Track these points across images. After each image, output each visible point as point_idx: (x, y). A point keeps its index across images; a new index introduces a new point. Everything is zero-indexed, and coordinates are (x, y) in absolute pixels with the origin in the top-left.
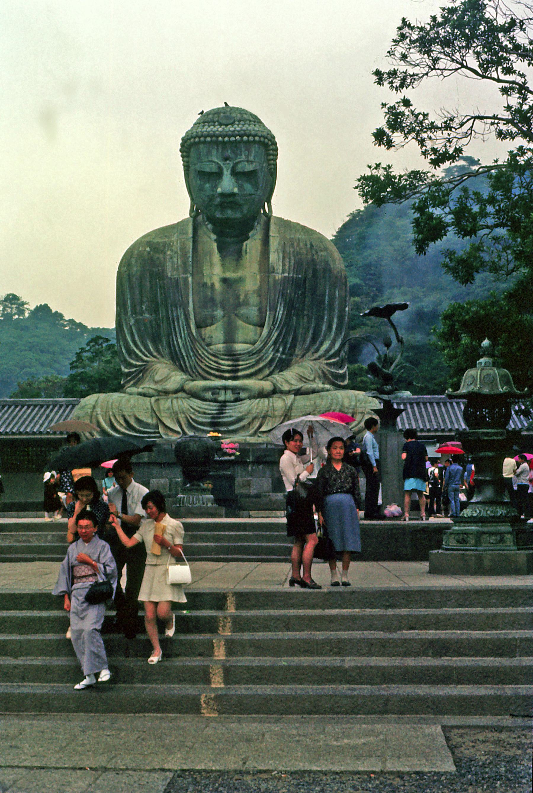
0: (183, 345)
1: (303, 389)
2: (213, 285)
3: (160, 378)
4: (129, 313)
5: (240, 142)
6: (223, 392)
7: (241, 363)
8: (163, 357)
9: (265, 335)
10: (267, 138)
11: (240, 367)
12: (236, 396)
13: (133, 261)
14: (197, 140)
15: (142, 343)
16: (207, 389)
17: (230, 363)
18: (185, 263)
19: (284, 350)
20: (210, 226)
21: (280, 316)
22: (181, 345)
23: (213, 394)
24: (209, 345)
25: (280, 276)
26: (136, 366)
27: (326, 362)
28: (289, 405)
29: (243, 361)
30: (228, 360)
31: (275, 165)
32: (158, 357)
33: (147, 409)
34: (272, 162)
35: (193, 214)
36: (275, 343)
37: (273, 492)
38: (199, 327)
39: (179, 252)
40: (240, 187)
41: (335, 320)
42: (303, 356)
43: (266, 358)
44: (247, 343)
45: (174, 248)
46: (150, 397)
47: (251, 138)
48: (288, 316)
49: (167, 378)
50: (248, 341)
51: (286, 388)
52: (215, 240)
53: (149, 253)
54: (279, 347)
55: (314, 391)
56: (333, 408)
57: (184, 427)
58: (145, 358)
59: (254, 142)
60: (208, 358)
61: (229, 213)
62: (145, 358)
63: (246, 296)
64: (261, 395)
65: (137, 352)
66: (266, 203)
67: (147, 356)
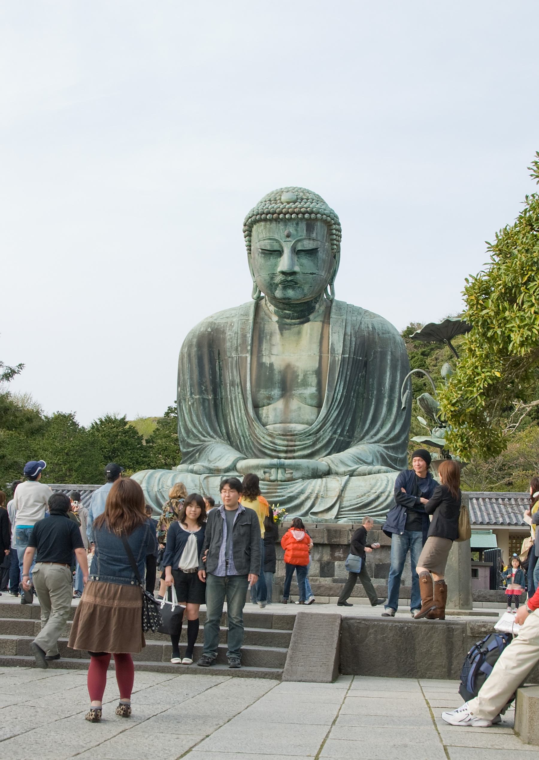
0: (239, 424)
1: (359, 470)
2: (271, 365)
3: (214, 458)
4: (189, 394)
5: (301, 219)
6: (273, 471)
8: (220, 437)
9: (323, 416)
10: (329, 216)
11: (296, 448)
13: (195, 340)
14: (258, 217)
17: (285, 443)
19: (342, 431)
20: (272, 308)
21: (339, 397)
23: (265, 473)
24: (264, 425)
25: (340, 357)
26: (194, 446)
27: (385, 445)
28: (342, 485)
29: (300, 441)
30: (284, 440)
31: (339, 246)
33: (196, 486)
34: (335, 242)
35: (255, 296)
36: (333, 424)
37: (321, 577)
39: (239, 332)
40: (301, 265)
41: (396, 404)
43: (323, 439)
44: (303, 423)
46: (201, 474)
47: (313, 216)
48: (347, 398)
49: (220, 458)
50: (305, 421)
51: (342, 469)
52: (277, 322)
53: (210, 333)
54: (336, 430)
55: (370, 474)
56: (388, 489)
58: (203, 438)
59: (316, 219)
60: (263, 437)
61: (290, 293)
62: (203, 438)
63: (305, 375)
64: (316, 474)
65: (194, 430)
66: (329, 287)
67: (204, 436)
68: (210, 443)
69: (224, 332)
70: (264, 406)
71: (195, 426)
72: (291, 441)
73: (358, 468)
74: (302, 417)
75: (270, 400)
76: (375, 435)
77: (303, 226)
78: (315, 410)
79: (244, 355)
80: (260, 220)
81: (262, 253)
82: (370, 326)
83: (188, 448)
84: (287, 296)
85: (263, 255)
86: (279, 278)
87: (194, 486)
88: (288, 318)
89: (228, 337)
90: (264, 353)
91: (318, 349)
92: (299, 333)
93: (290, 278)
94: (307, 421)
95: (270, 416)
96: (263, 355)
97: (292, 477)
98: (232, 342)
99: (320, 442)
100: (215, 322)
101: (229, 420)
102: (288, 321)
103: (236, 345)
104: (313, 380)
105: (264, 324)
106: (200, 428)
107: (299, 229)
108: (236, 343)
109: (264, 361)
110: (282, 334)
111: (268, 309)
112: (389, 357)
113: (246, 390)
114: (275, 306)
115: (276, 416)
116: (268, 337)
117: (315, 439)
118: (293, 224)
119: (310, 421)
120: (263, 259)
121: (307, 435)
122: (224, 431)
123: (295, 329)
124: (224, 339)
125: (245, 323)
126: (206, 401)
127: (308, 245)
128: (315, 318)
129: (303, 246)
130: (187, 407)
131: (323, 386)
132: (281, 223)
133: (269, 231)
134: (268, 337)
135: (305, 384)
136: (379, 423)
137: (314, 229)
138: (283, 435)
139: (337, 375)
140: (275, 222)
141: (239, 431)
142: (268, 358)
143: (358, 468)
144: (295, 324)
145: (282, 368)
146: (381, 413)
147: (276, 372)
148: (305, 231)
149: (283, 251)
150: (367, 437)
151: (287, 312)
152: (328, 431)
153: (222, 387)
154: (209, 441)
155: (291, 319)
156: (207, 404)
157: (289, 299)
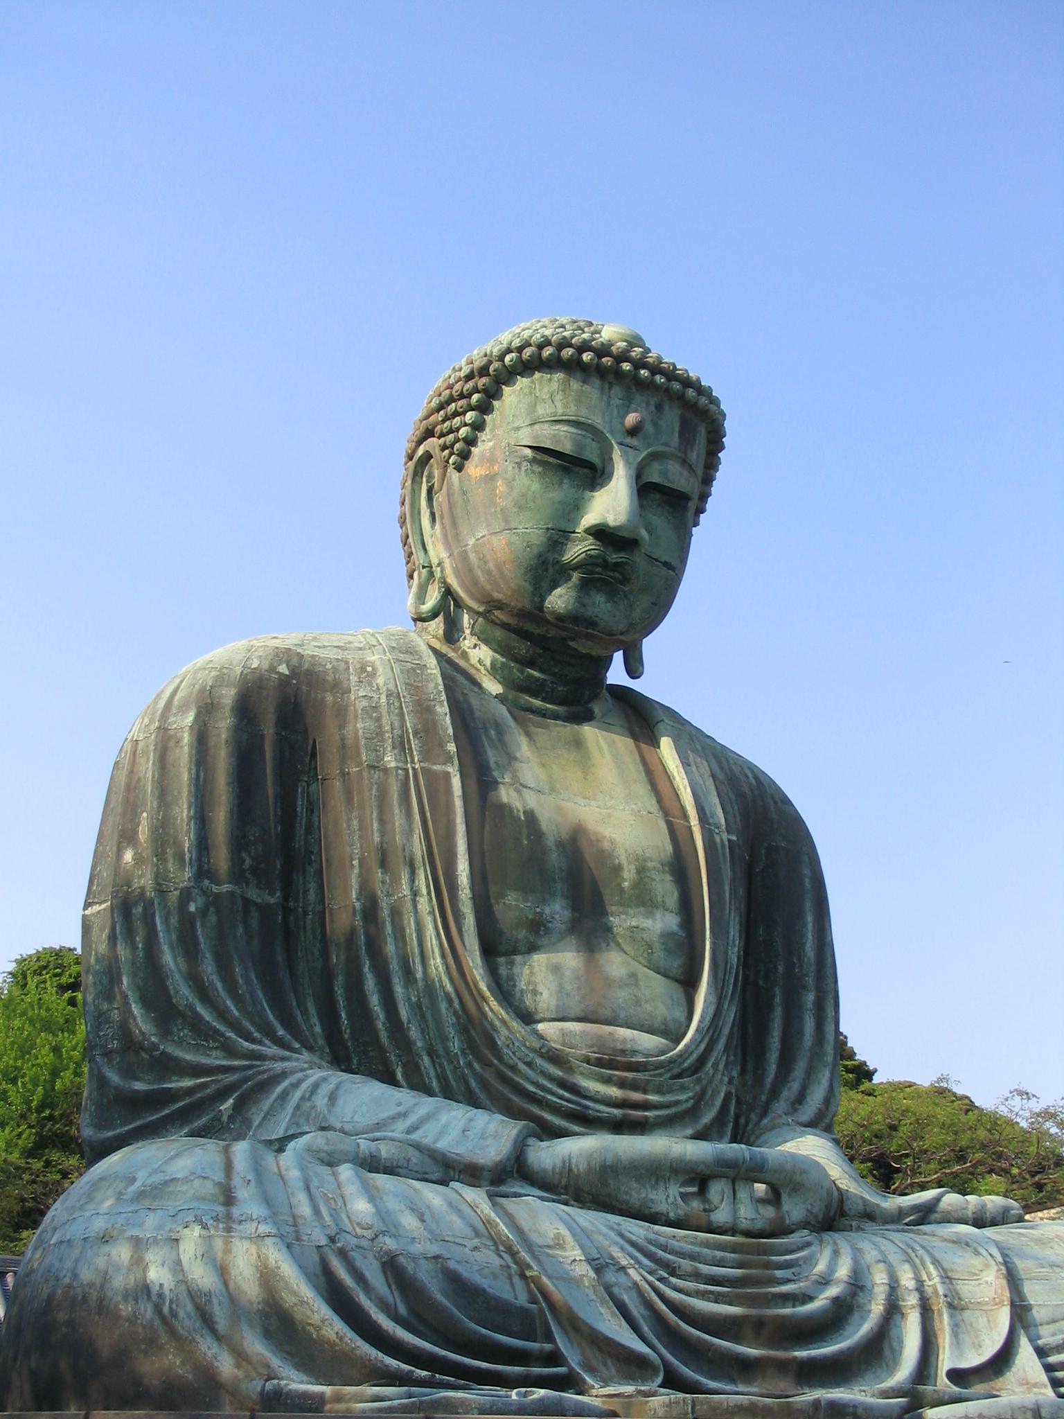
0: (417, 1008)
2: (531, 817)
7: (653, 1098)
8: (310, 1049)
12: (769, 1212)
15: (232, 990)
16: (657, 1171)
17: (614, 1092)
18: (428, 729)
22: (404, 1012)
26: (197, 1070)
28: (1000, 1259)
29: (659, 1091)
30: (607, 1081)
32: (297, 1046)
38: (492, 948)
42: (764, 1114)
45: (380, 681)
50: (657, 1023)
53: (284, 682)
57: (646, 1329)
60: (529, 1064)
61: (600, 605)
63: (641, 870)
68: (286, 1064)
69: (338, 687)
70: (514, 951)
71: (204, 994)
72: (634, 1086)
73: (938, 1199)
74: (648, 1008)
75: (537, 933)
76: (800, 1099)
77: (672, 417)
78: (678, 992)
79: (436, 768)
80: (553, 365)
81: (534, 461)
82: (750, 775)
83: (162, 1079)
84: (590, 612)
85: (538, 469)
86: (578, 549)
87: (468, 1231)
88: (534, 694)
89: (365, 703)
90: (495, 774)
91: (654, 801)
92: (578, 744)
93: (614, 557)
94: (665, 1021)
95: (540, 988)
96: (497, 783)
97: (782, 1220)
98: (378, 719)
99: (707, 1104)
100: (299, 650)
101: (339, 992)
102: (537, 703)
103: (397, 732)
104: (665, 888)
105: (465, 695)
106: (229, 1003)
107: (661, 422)
108: (396, 724)
109: (505, 799)
110: (528, 735)
111: (465, 655)
112: (806, 871)
113: (453, 887)
114: (499, 648)
115: (561, 987)
116: (493, 733)
117: (698, 1088)
118: (648, 403)
119: (671, 1025)
120: (536, 479)
121: (676, 1071)
122: (318, 1029)
123: (564, 730)
124: (342, 712)
125: (415, 672)
126: (253, 909)
127: (677, 477)
128: (604, 715)
129: (664, 473)
130: (174, 921)
131: (697, 917)
132: (617, 391)
133: (578, 402)
134: (493, 733)
135: (643, 899)
136: (801, 1066)
137: (695, 439)
138: (599, 1063)
139: (727, 888)
140: (597, 382)
141: (414, 1033)
142: (514, 794)
143: (938, 1199)
144: (556, 717)
145: (564, 834)
146: (801, 1033)
147: (550, 842)
148: (676, 435)
149: (603, 472)
150: (780, 1107)
151: (536, 674)
152: (721, 1067)
153: (311, 870)
154: (283, 1059)
155: (544, 700)
156: (254, 923)
157: (591, 623)
